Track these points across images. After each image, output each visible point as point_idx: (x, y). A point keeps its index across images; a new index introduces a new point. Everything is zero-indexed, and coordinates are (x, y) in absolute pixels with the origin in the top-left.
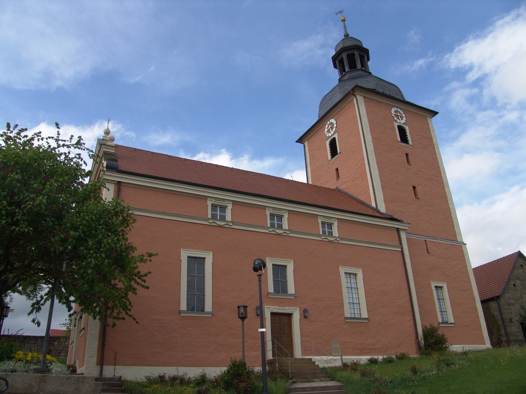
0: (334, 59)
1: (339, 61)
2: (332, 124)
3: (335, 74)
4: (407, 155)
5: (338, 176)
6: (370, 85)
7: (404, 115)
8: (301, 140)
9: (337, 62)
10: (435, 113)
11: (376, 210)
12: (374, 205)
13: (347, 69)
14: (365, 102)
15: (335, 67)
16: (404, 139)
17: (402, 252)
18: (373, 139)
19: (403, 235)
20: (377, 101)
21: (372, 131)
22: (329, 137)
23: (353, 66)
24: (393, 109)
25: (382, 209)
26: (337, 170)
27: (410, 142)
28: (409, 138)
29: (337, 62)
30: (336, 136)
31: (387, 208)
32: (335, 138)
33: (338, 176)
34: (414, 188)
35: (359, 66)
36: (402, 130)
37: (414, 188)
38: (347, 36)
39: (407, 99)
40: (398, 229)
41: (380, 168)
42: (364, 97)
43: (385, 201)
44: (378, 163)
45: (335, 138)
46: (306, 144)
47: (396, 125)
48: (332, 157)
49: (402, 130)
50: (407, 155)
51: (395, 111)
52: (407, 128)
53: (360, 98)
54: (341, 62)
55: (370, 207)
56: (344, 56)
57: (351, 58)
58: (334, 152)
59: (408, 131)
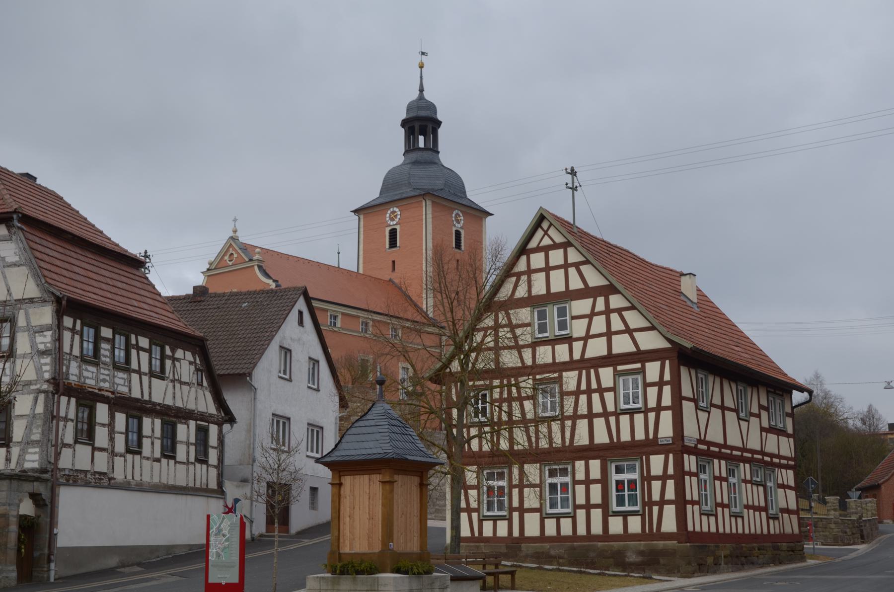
0: (404, 123)
2: (394, 212)
5: (394, 269)
11: (426, 313)
12: (424, 307)
26: (394, 262)
27: (463, 248)
28: (463, 244)
30: (398, 227)
33: (394, 269)
36: (458, 234)
38: (421, 97)
47: (454, 229)
48: (390, 247)
49: (458, 234)
51: (457, 214)
52: (462, 232)
53: (429, 203)
58: (393, 243)
59: (463, 236)
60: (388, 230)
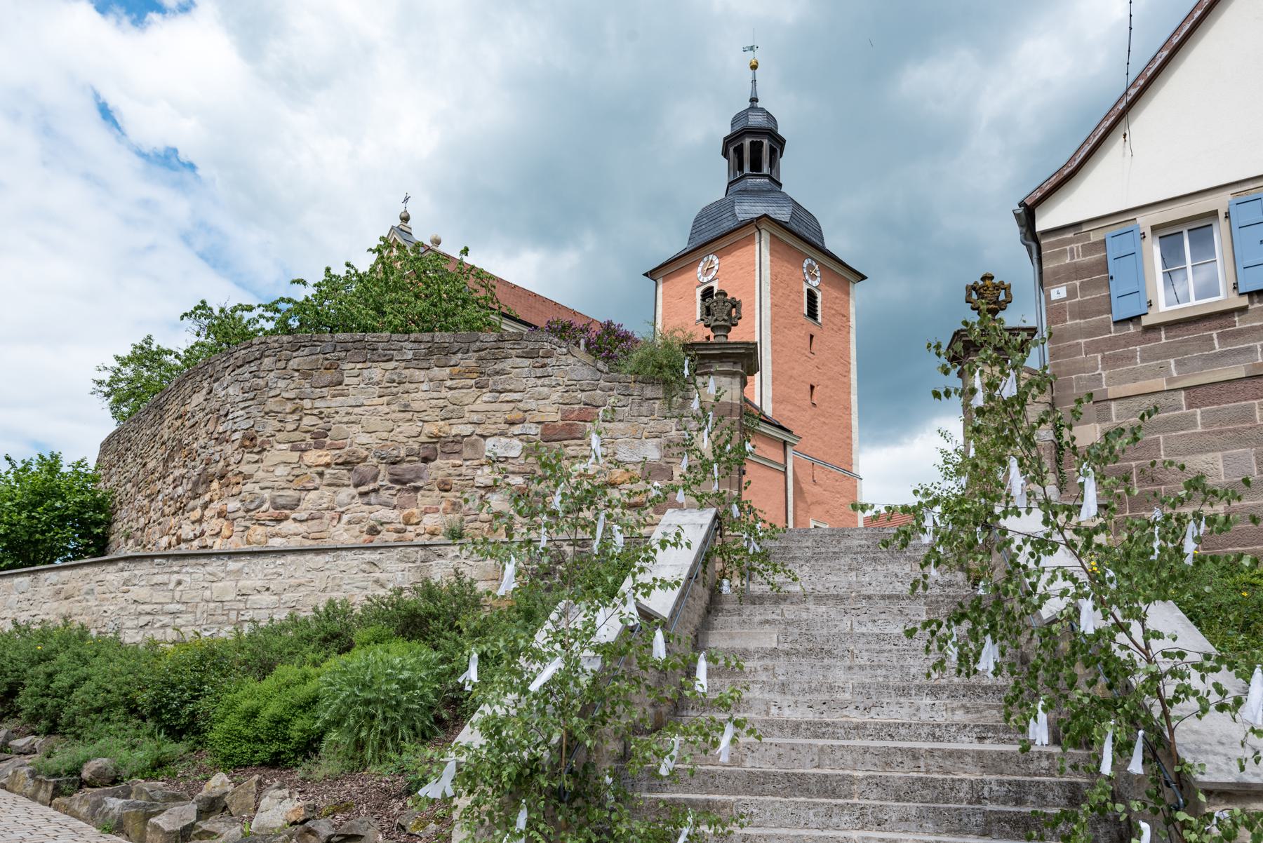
0: (728, 141)
1: (735, 150)
3: (721, 168)
4: (812, 337)
6: (783, 214)
7: (818, 274)
8: (651, 274)
9: (731, 150)
10: (863, 278)
11: (760, 409)
12: (757, 403)
13: (747, 170)
14: (772, 243)
15: (725, 154)
16: (812, 313)
17: (785, 473)
18: (774, 305)
19: (789, 450)
20: (788, 245)
21: (773, 292)
22: (703, 283)
23: (756, 166)
24: (807, 262)
25: (768, 410)
27: (820, 320)
28: (819, 313)
29: (731, 150)
31: (774, 410)
32: (712, 288)
34: (812, 387)
35: (766, 170)
36: (812, 297)
37: (812, 387)
39: (830, 245)
40: (785, 443)
41: (774, 351)
42: (772, 235)
43: (774, 401)
44: (773, 343)
45: (712, 288)
46: (660, 281)
47: (806, 287)
49: (812, 297)
50: (812, 337)
51: (810, 267)
52: (819, 295)
54: (739, 151)
55: (753, 405)
56: (747, 142)
57: (754, 148)
59: (819, 300)
60: (699, 292)
